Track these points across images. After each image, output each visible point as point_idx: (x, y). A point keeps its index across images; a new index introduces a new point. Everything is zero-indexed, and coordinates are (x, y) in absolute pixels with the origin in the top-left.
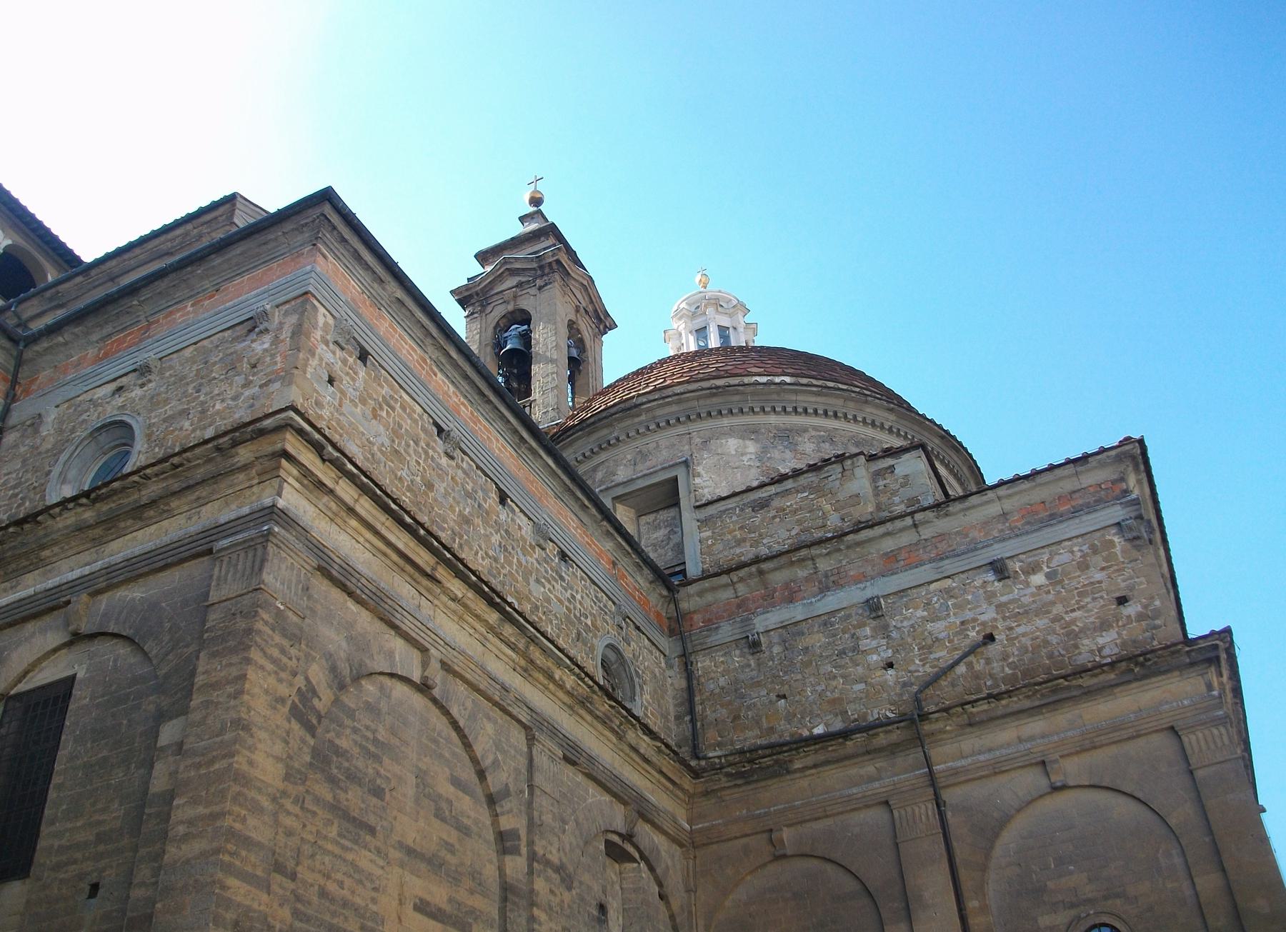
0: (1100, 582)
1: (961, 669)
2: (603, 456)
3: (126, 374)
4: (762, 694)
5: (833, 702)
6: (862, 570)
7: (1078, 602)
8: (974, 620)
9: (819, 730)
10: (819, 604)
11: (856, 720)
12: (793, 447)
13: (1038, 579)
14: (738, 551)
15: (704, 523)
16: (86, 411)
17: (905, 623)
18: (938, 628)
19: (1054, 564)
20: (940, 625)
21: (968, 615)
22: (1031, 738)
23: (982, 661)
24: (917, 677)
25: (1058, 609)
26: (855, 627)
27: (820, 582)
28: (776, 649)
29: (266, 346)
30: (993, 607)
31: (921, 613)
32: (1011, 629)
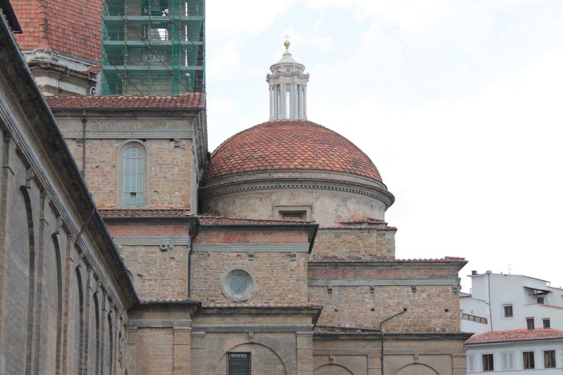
0: (442, 302)
1: (395, 318)
2: (276, 190)
3: (241, 252)
4: (330, 307)
5: (353, 317)
6: (369, 273)
7: (434, 307)
8: (402, 303)
9: (347, 326)
10: (353, 282)
11: (359, 325)
12: (346, 205)
13: (424, 295)
14: (327, 251)
16: (227, 260)
17: (381, 297)
19: (430, 292)
20: (391, 301)
21: (401, 301)
22: (412, 347)
23: (402, 317)
24: (381, 317)
25: (428, 307)
26: (364, 293)
27: (355, 273)
28: (337, 293)
29: (295, 265)
30: (409, 300)
31: (386, 295)
32: (412, 309)
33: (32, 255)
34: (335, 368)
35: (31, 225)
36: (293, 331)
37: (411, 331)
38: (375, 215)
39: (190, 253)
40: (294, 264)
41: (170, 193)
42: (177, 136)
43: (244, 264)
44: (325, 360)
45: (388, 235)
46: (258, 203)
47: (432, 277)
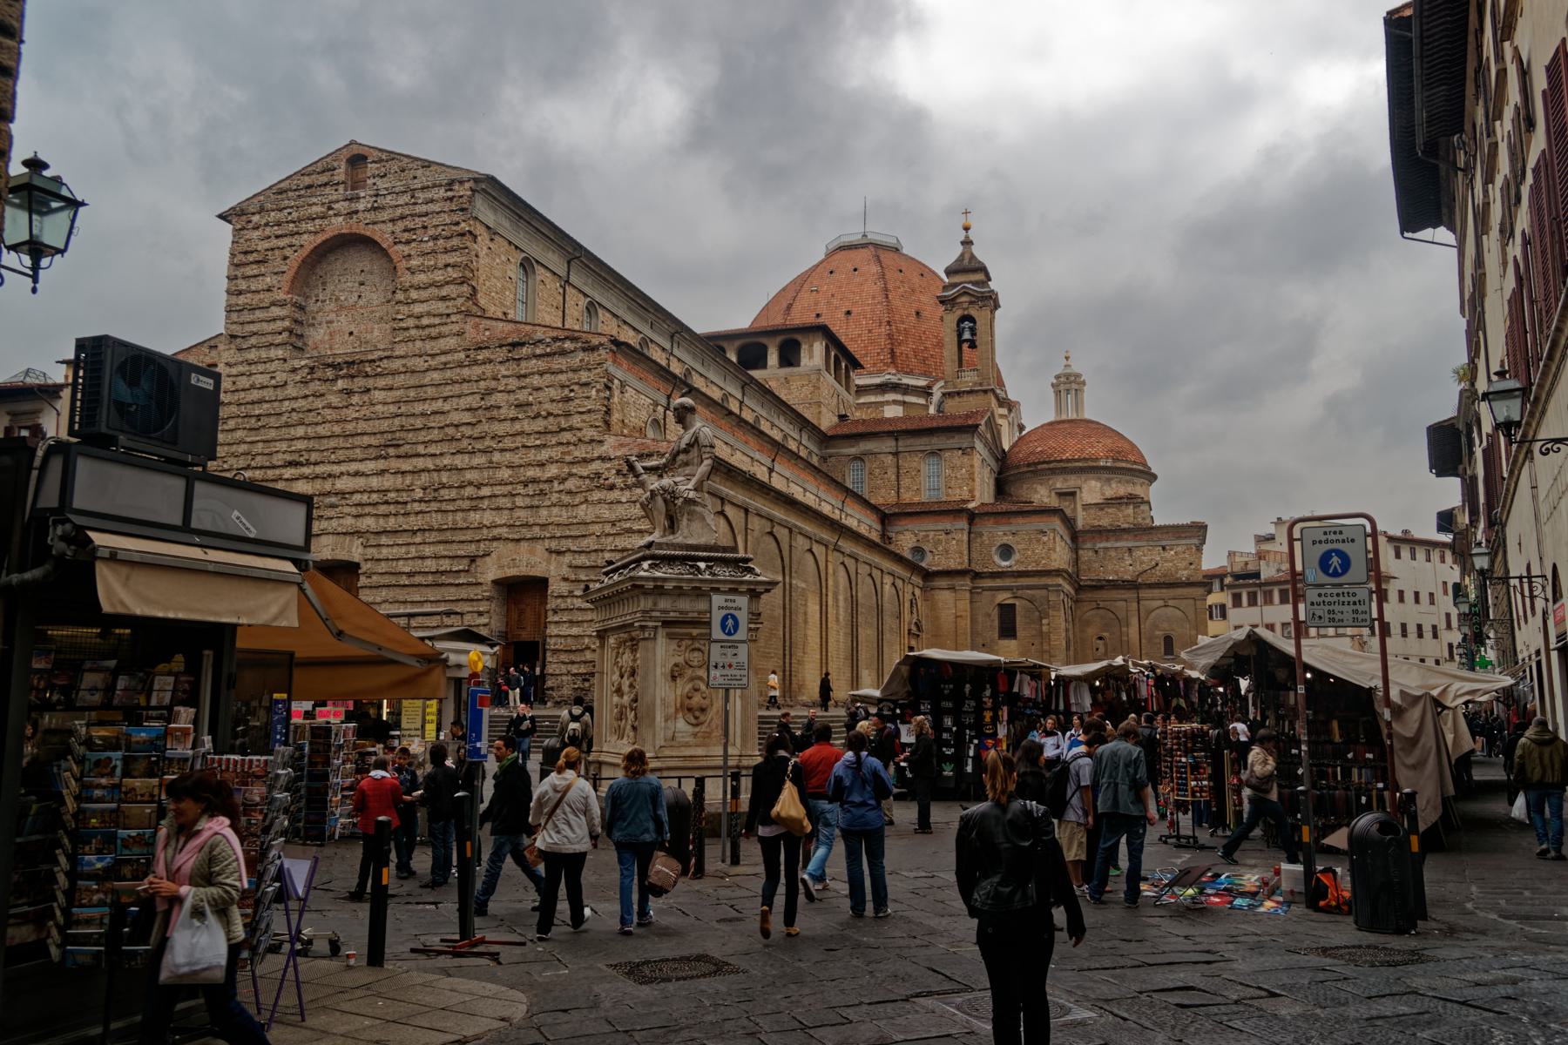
15: (1084, 510)
18: (1145, 559)
33: (784, 568)
34: (1101, 611)
35: (780, 551)
36: (1045, 587)
37: (1162, 580)
38: (1138, 490)
39: (970, 533)
40: (1045, 539)
41: (960, 488)
42: (964, 446)
43: (1008, 540)
44: (1094, 605)
45: (1144, 507)
46: (1039, 488)
47: (1179, 538)
